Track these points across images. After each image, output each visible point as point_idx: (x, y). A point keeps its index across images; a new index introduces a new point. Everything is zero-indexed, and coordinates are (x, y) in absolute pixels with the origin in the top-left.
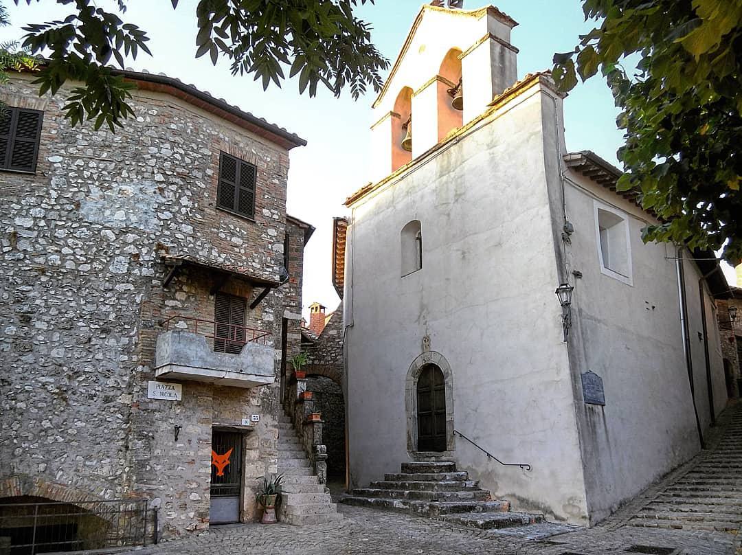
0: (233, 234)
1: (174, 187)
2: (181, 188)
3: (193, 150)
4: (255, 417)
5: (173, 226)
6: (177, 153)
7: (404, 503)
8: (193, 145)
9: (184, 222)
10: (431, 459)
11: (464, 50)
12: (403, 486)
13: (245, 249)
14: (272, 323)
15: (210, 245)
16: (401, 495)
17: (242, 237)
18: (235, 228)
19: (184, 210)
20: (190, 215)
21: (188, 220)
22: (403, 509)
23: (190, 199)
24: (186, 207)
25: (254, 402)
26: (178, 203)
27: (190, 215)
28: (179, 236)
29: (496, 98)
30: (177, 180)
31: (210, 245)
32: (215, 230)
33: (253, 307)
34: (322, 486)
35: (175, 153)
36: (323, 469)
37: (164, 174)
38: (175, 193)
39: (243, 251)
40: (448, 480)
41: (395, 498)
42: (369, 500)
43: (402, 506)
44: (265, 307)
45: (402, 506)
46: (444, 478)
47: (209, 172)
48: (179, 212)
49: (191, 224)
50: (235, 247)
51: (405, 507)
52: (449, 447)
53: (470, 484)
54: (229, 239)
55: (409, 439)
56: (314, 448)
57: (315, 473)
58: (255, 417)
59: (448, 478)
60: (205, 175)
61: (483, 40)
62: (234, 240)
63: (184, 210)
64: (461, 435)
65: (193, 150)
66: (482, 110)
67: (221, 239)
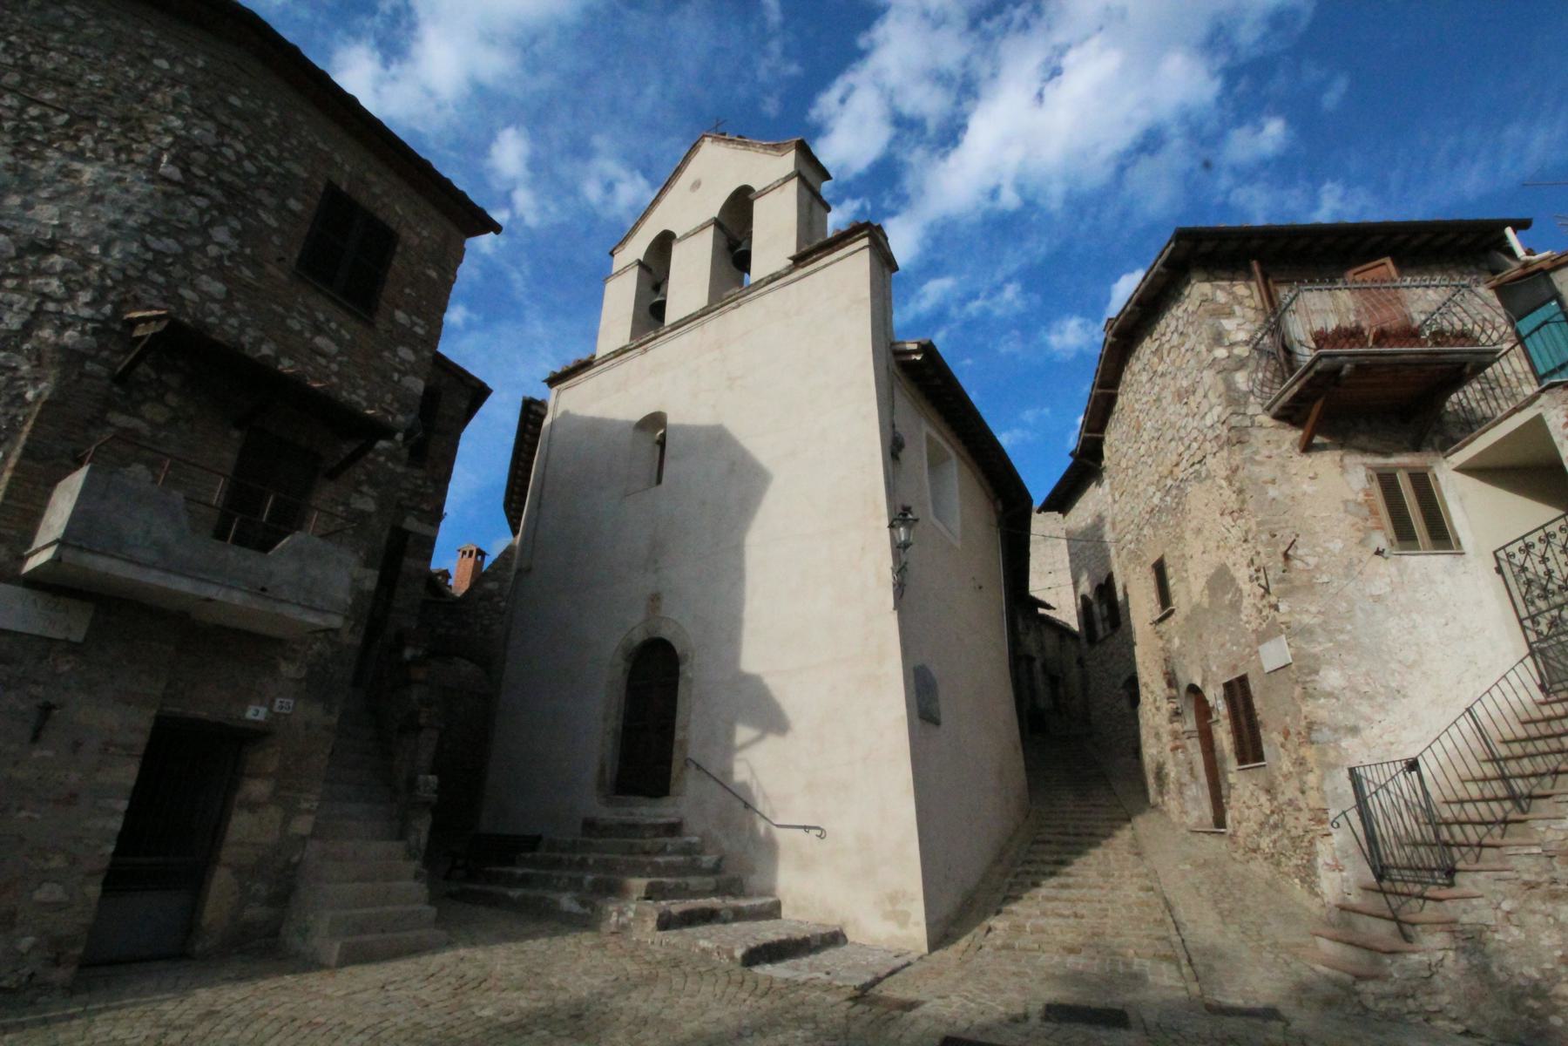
0: (318, 329)
1: (202, 202)
2: (220, 207)
3: (268, 156)
4: (284, 704)
5: (178, 271)
6: (229, 146)
7: (583, 904)
8: (270, 147)
9: (207, 271)
10: (648, 812)
11: (757, 187)
12: (582, 865)
13: (340, 364)
14: (370, 515)
15: (259, 334)
16: (576, 884)
17: (339, 342)
18: (328, 320)
19: (213, 250)
20: (227, 263)
21: (218, 269)
22: (577, 914)
23: (235, 234)
24: (222, 245)
25: (288, 670)
26: (204, 230)
27: (227, 263)
28: (187, 293)
29: (805, 248)
30: (216, 192)
31: (259, 334)
32: (280, 310)
33: (332, 475)
34: (415, 865)
35: (223, 144)
36: (422, 827)
37: (185, 171)
38: (202, 212)
39: (334, 367)
40: (670, 854)
41: (565, 890)
42: (511, 893)
43: (575, 908)
44: (360, 483)
45: (575, 908)
46: (662, 851)
47: (293, 204)
48: (202, 248)
49: (225, 280)
50: (316, 345)
51: (581, 911)
52: (674, 789)
53: (708, 860)
54: (307, 335)
55: (602, 771)
56: (411, 783)
57: (401, 835)
58: (284, 704)
59: (669, 848)
60: (282, 206)
61: (787, 179)
62: (320, 341)
63: (213, 250)
64: (698, 767)
65: (268, 156)
66: (781, 261)
67: (290, 330)
